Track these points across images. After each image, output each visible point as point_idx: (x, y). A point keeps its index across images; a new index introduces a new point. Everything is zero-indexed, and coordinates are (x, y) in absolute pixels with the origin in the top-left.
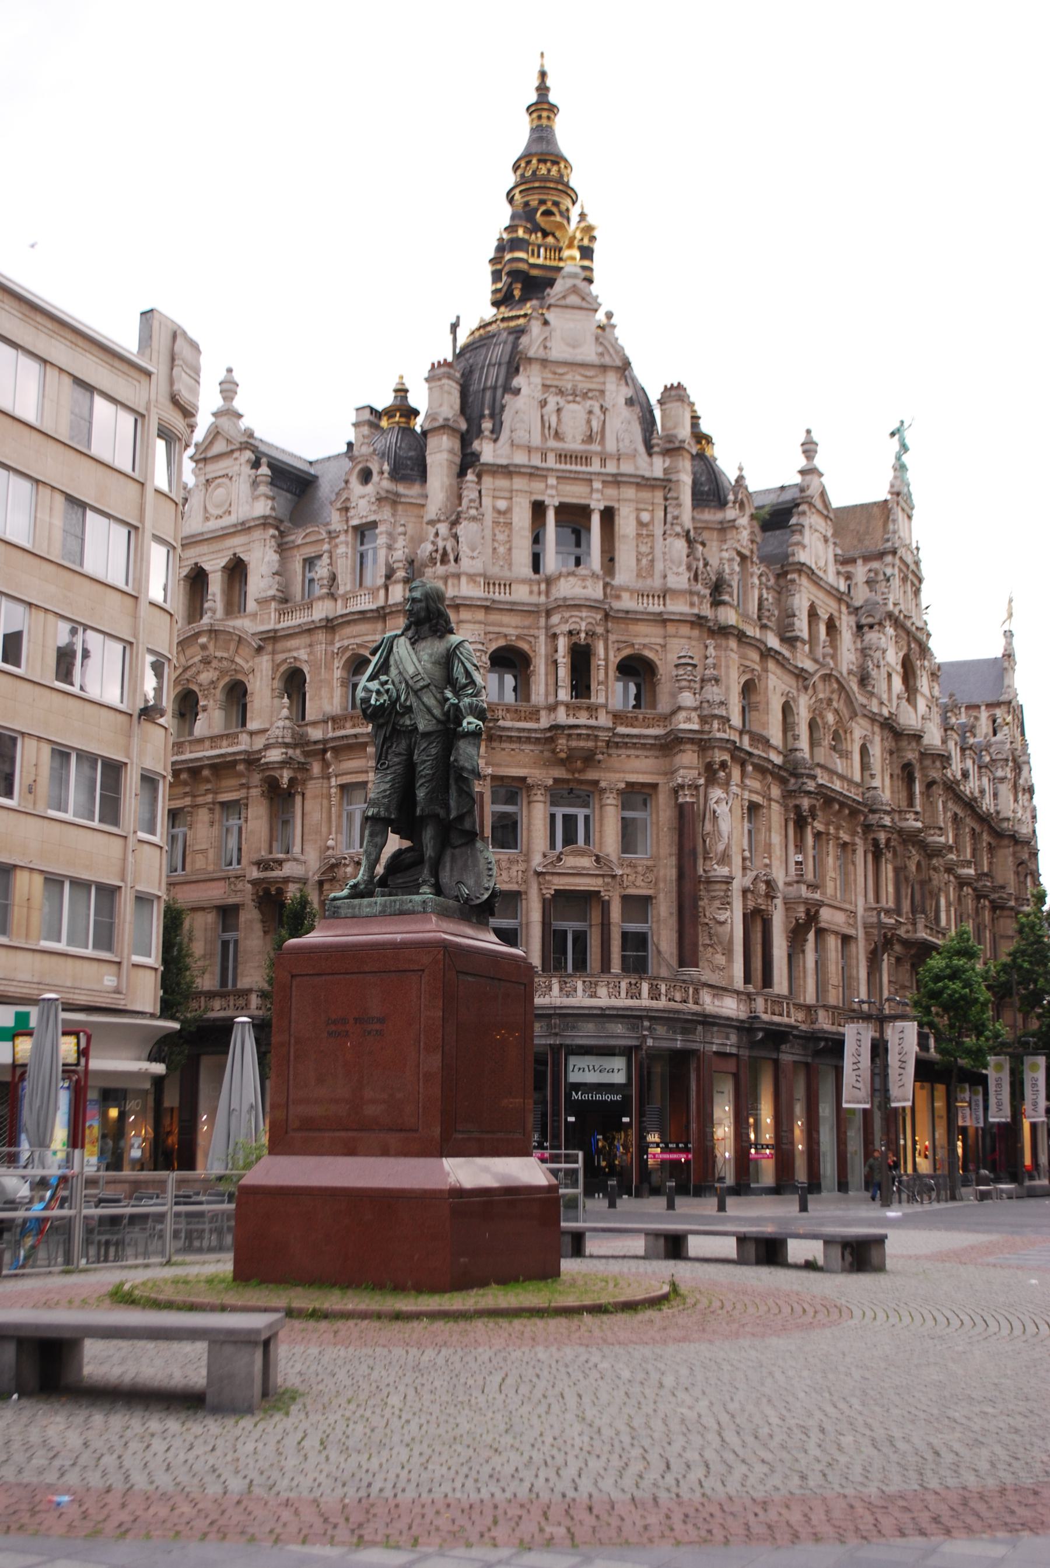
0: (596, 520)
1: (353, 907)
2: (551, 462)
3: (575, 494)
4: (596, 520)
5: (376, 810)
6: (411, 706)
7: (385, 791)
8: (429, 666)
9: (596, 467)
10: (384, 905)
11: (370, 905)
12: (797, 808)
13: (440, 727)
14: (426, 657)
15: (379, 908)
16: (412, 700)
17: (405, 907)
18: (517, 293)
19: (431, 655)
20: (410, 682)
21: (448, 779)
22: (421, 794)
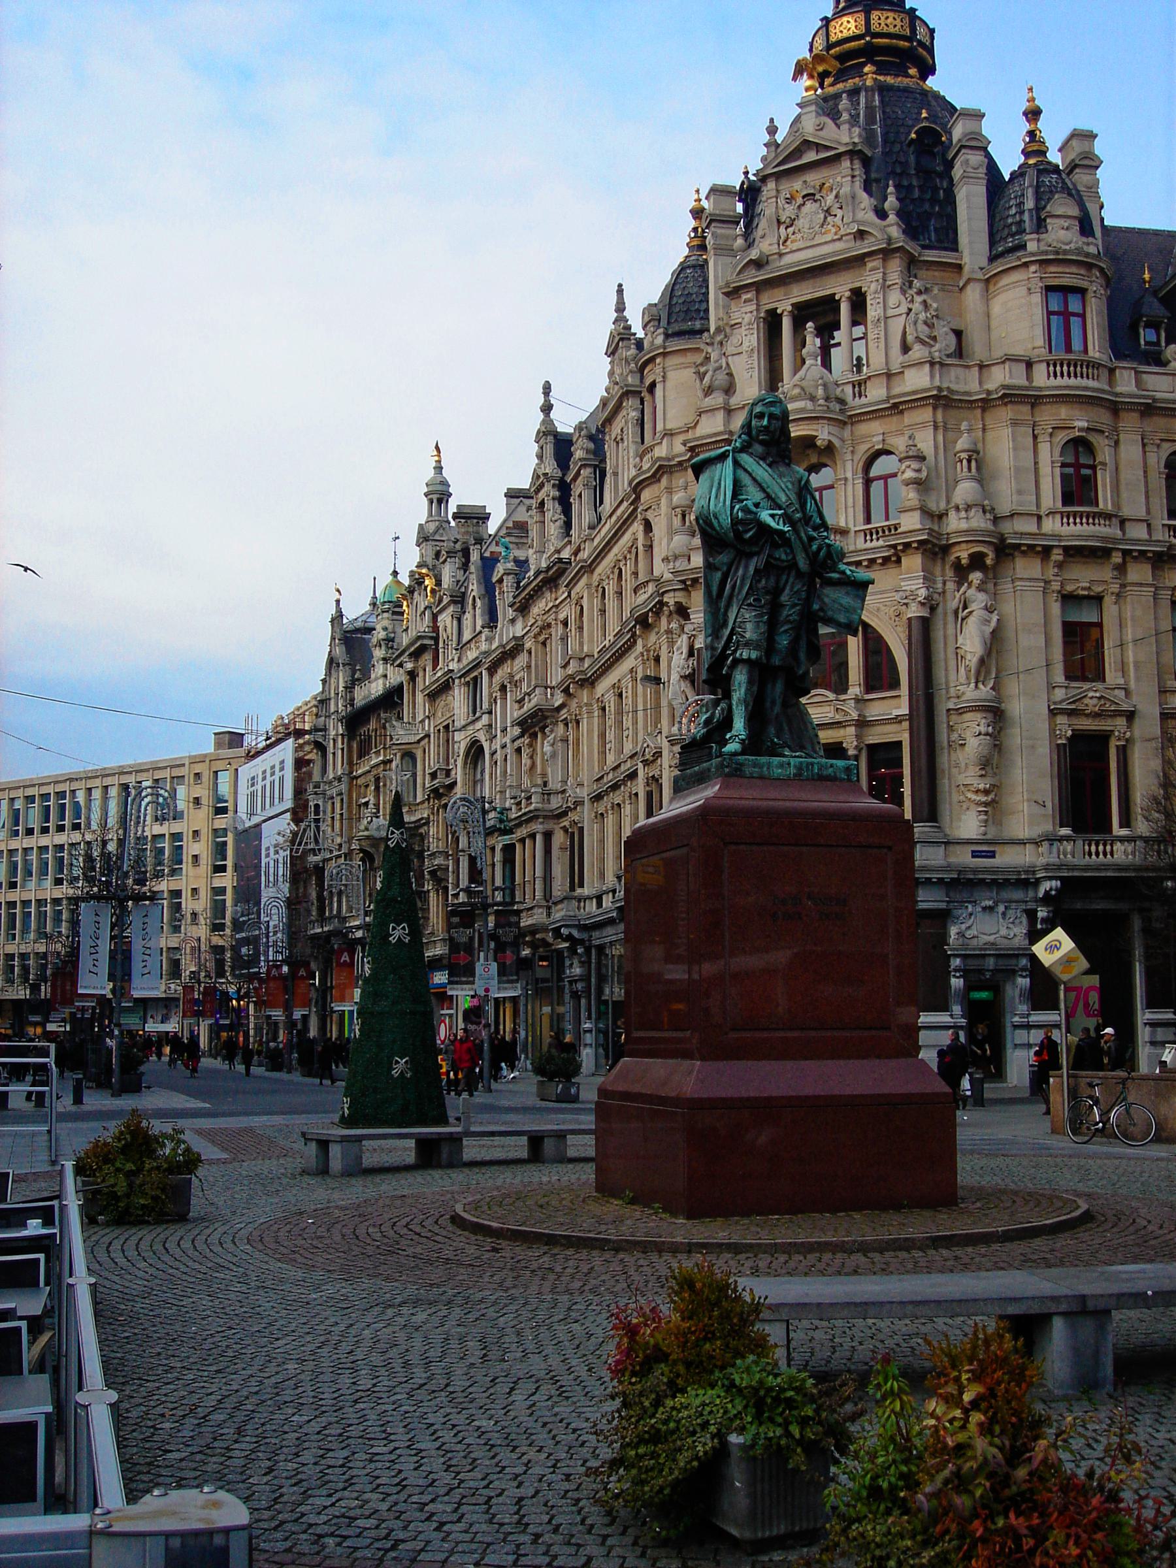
1: (761, 766)
6: (789, 539)
10: (799, 768)
11: (781, 766)
14: (790, 486)
15: (793, 771)
19: (793, 484)
22: (784, 641)
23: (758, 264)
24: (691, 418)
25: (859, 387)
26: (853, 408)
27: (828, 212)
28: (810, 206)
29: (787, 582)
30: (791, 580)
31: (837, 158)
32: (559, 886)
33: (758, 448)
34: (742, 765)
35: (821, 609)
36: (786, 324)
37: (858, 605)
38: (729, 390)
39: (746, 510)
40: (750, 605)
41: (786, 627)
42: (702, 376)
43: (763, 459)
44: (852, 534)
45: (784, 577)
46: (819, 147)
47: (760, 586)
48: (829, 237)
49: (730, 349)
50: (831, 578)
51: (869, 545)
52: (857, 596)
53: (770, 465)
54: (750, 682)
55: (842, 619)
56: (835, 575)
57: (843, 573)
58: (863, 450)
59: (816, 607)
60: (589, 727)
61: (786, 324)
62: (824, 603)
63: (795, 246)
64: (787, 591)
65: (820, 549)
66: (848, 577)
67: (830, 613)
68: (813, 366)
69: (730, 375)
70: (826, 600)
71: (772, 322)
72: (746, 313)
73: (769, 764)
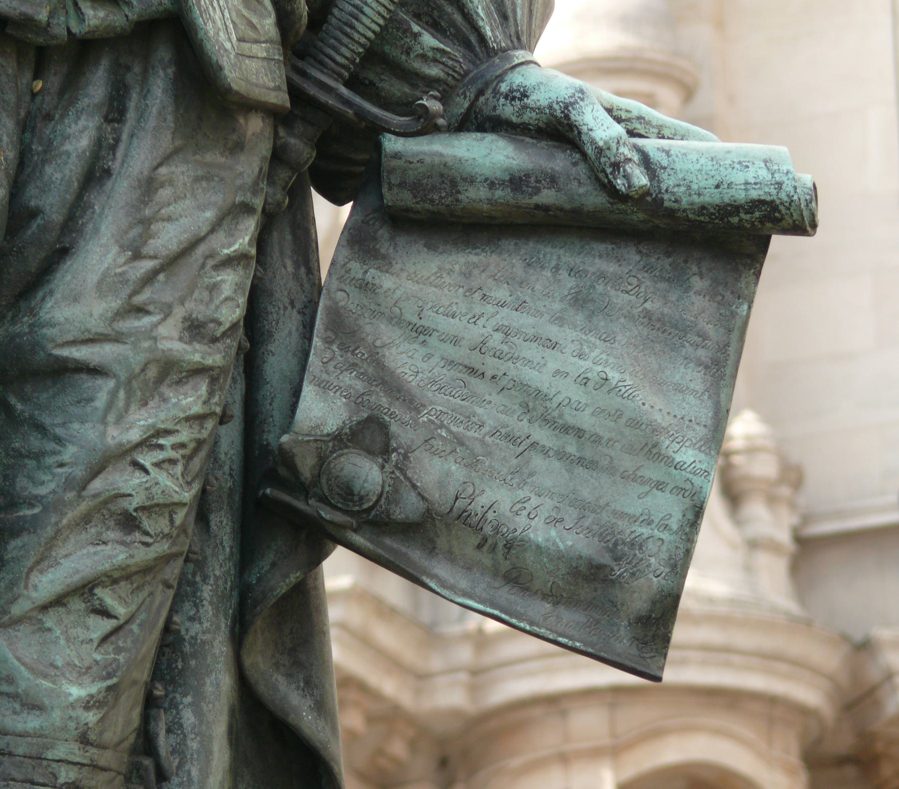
29: (95, 175)
30: (137, 157)
35: (368, 433)
37: (666, 399)
41: (80, 558)
45: (79, 135)
50: (451, 178)
52: (667, 332)
55: (538, 513)
56: (486, 155)
59: (320, 410)
62: (394, 387)
64: (99, 257)
66: (599, 167)
67: (437, 474)
70: (406, 360)
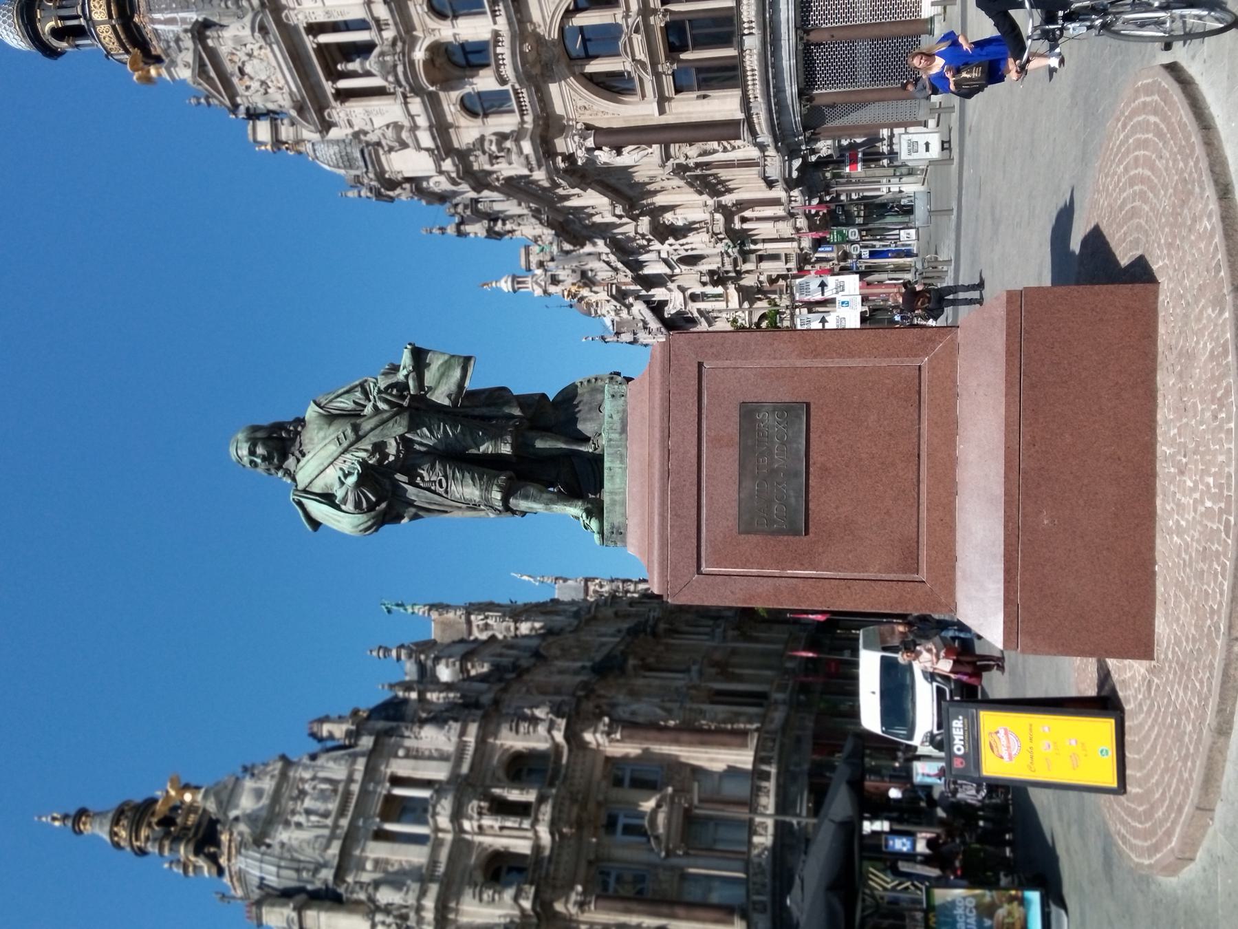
0: (398, 792)
1: (614, 503)
2: (344, 822)
3: (377, 806)
4: (398, 792)
5: (495, 488)
7: (473, 479)
8: (332, 428)
9: (355, 788)
12: (635, 667)
13: (406, 415)
14: (322, 434)
15: (617, 464)
16: (367, 444)
17: (618, 426)
18: (212, 850)
19: (320, 429)
20: (345, 444)
21: (475, 417)
23: (301, 109)
24: (425, 154)
25: (380, 25)
26: (398, 31)
27: (250, 55)
28: (248, 69)
29: (421, 444)
31: (206, 47)
32: (779, 211)
33: (290, 463)
34: (613, 527)
35: (449, 396)
36: (343, 84)
38: (397, 127)
39: (344, 501)
40: (447, 492)
42: (391, 149)
43: (298, 461)
44: (496, 27)
46: (202, 65)
47: (427, 479)
48: (271, 55)
49: (368, 128)
51: (503, 12)
53: (304, 455)
54: (526, 497)
56: (411, 383)
57: (407, 377)
58: (433, 23)
60: (660, 200)
61: (343, 84)
63: (282, 82)
65: (386, 401)
68: (371, 63)
69: (388, 126)
71: (344, 96)
72: (338, 112)
73: (611, 493)
